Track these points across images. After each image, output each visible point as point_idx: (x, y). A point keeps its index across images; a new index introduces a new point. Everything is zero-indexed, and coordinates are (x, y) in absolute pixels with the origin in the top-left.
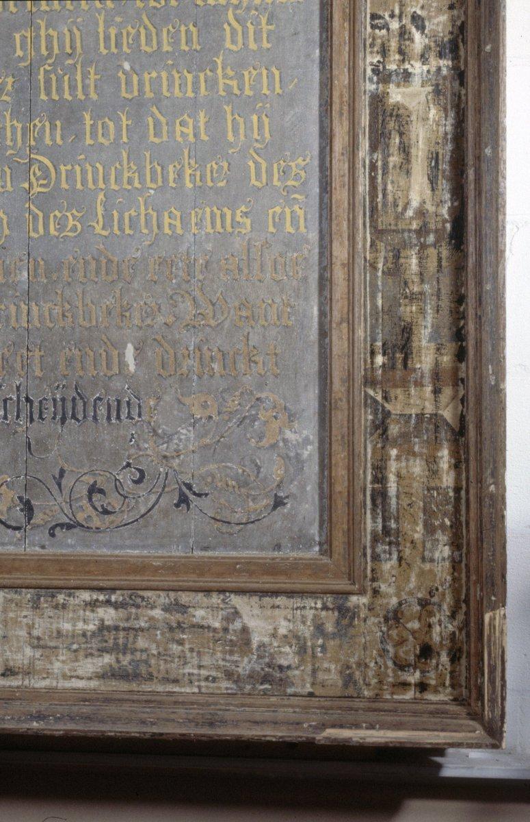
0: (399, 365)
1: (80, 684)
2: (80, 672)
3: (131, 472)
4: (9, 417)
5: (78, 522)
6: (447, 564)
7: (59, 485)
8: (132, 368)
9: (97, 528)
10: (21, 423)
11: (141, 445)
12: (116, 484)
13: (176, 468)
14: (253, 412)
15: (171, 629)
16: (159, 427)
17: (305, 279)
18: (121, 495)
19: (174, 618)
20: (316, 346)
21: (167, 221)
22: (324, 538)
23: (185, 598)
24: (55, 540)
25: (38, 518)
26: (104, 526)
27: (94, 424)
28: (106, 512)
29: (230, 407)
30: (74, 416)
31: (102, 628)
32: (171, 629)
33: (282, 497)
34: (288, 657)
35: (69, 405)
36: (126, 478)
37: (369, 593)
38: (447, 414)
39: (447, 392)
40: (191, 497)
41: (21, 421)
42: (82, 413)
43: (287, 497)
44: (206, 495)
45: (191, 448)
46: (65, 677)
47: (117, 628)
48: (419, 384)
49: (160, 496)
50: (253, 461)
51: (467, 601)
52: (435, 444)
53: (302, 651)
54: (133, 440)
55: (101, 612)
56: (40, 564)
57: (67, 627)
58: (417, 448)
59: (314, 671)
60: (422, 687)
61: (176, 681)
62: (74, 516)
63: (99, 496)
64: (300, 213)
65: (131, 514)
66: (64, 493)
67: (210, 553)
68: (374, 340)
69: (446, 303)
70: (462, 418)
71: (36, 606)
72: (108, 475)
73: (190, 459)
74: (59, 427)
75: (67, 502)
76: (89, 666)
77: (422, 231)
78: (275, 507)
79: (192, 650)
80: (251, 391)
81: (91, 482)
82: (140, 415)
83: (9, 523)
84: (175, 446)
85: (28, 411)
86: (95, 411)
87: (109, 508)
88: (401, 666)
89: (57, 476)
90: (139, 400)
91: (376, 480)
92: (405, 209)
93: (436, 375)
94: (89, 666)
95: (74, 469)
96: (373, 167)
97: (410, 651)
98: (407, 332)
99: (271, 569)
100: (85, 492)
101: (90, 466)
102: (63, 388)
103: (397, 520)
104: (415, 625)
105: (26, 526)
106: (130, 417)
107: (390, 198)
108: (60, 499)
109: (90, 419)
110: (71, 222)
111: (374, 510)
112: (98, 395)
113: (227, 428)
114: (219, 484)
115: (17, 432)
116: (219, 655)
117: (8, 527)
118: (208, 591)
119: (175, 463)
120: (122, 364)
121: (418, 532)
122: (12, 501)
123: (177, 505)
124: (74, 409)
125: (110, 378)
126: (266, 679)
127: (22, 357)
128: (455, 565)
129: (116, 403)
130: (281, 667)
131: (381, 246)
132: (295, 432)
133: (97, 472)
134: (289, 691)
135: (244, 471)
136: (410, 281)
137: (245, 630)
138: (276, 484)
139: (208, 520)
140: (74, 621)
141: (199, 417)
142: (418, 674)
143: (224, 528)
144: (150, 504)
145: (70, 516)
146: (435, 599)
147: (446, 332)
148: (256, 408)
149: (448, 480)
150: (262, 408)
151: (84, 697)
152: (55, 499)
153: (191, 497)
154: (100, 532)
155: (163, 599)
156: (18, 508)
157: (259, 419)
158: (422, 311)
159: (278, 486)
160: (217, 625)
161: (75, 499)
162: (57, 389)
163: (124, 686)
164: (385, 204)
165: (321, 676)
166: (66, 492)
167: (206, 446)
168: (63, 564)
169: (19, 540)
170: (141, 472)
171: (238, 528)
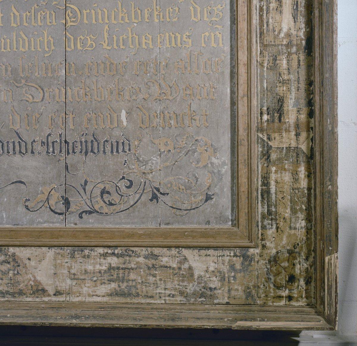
0: (277, 120)
1: (98, 299)
2: (98, 293)
3: (125, 181)
4: (56, 151)
5: (95, 210)
6: (304, 230)
7: (85, 190)
8: (125, 123)
9: (106, 213)
10: (63, 155)
11: (130, 167)
12: (116, 189)
13: (150, 179)
14: (194, 148)
15: (149, 268)
16: (141, 157)
17: (223, 73)
18: (120, 195)
19: (150, 262)
20: (229, 110)
21: (144, 41)
22: (234, 217)
23: (156, 251)
24: (83, 220)
25: (73, 208)
27: (104, 155)
28: (111, 204)
29: (180, 145)
30: (92, 151)
31: (110, 268)
32: (149, 268)
33: (210, 194)
34: (215, 283)
35: (89, 145)
37: (260, 247)
38: (304, 147)
39: (304, 135)
40: (159, 195)
41: (62, 154)
42: (97, 149)
43: (213, 195)
44: (168, 194)
45: (159, 168)
46: (89, 295)
47: (118, 268)
48: (288, 131)
49: (142, 195)
51: (315, 251)
52: (297, 163)
53: (223, 279)
54: (126, 164)
55: (109, 259)
56: (74, 233)
57: (90, 268)
58: (286, 167)
59: (229, 291)
60: (290, 298)
61: (152, 297)
62: (93, 206)
63: (107, 195)
64: (220, 36)
65: (125, 205)
67: (170, 227)
68: (262, 106)
69: (303, 86)
70: (312, 150)
71: (73, 257)
72: (112, 184)
74: (84, 157)
75: (89, 199)
76: (103, 289)
77: (289, 45)
78: (206, 201)
79: (161, 280)
80: (192, 136)
82: (129, 150)
84: (150, 167)
85: (66, 148)
86: (104, 148)
87: (113, 202)
88: (278, 287)
90: (129, 141)
91: (263, 184)
92: (279, 33)
93: (297, 126)
94: (103, 289)
95: (93, 181)
96: (261, 9)
97: (283, 279)
98: (281, 101)
99: (205, 234)
100: (99, 193)
101: (102, 179)
103: (276, 206)
104: (286, 264)
105: (66, 212)
106: (124, 151)
107: (271, 27)
108: (85, 197)
109: (102, 152)
110: (89, 42)
111: (262, 201)
112: (106, 139)
114: (175, 188)
115: (60, 160)
116: (176, 282)
117: (56, 213)
118: (169, 247)
119: (150, 176)
120: (119, 121)
121: (287, 213)
122: (58, 199)
123: (151, 200)
124: (92, 147)
125: (112, 129)
126: (202, 295)
127: (62, 118)
128: (308, 231)
130: (211, 289)
131: (266, 53)
132: (218, 159)
133: (106, 182)
134: (215, 301)
135: (189, 181)
136: (282, 73)
137: (190, 268)
138: (207, 187)
139: (169, 207)
140: (94, 265)
142: (287, 291)
143: (178, 212)
144: (136, 200)
145: (91, 206)
146: (297, 250)
147: (303, 102)
149: (304, 183)
150: (199, 145)
151: (101, 306)
152: (82, 197)
153: (159, 195)
155: (144, 251)
156: (61, 203)
157: (197, 151)
158: (289, 90)
159: (208, 188)
160: (175, 266)
162: (82, 136)
163: (122, 300)
164: (268, 31)
165: (233, 293)
166: (88, 193)
167: (167, 167)
168: (86, 233)
169: (62, 220)
170: (131, 181)
171: (186, 212)
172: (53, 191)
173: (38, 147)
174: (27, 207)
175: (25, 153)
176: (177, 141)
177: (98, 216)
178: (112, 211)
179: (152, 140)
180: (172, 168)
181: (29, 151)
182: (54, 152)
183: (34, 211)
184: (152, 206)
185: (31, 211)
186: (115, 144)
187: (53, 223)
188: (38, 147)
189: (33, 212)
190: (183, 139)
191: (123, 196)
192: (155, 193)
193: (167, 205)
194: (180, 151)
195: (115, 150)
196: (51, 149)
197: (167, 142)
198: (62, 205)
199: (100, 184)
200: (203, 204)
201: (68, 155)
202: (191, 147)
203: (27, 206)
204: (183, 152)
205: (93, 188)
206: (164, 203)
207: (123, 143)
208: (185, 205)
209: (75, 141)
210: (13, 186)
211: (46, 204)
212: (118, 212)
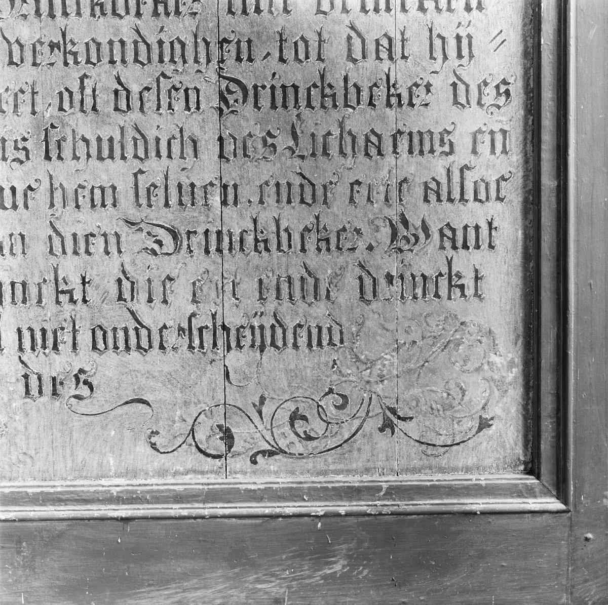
3: (334, 397)
4: (205, 345)
5: (281, 449)
9: (300, 454)
10: (219, 351)
11: (343, 371)
12: (318, 410)
13: (380, 393)
14: (458, 337)
16: (362, 353)
18: (324, 421)
22: (529, 457)
24: (257, 467)
26: (307, 451)
27: (295, 351)
28: (309, 438)
30: (273, 344)
35: (268, 333)
36: (329, 403)
40: (395, 421)
41: (218, 349)
42: (281, 340)
43: (492, 419)
44: (411, 418)
45: (395, 372)
49: (364, 420)
50: (458, 385)
54: (336, 366)
62: (276, 442)
63: (301, 422)
65: (334, 439)
66: (265, 420)
72: (311, 402)
73: (394, 384)
74: (258, 354)
78: (480, 429)
81: (293, 408)
82: (342, 342)
83: (208, 451)
84: (379, 372)
85: (225, 339)
86: (295, 338)
87: (313, 435)
89: (258, 404)
90: (341, 326)
101: (292, 393)
102: (261, 316)
105: (226, 454)
106: (331, 343)
108: (261, 427)
109: (290, 345)
112: (298, 322)
113: (431, 353)
114: (424, 408)
117: (208, 455)
122: (212, 429)
123: (381, 430)
124: (273, 336)
127: (217, 284)
129: (317, 330)
133: (299, 399)
135: (449, 394)
138: (481, 406)
139: (413, 443)
141: (403, 342)
144: (354, 429)
145: (272, 443)
148: (460, 333)
150: (466, 332)
152: (255, 426)
153: (395, 421)
154: (303, 458)
156: (218, 437)
159: (483, 408)
161: (277, 426)
162: (255, 317)
167: (409, 371)
169: (220, 468)
170: (344, 397)
171: (443, 450)
172: (202, 416)
173: (171, 338)
174: (153, 446)
175: (147, 348)
176: (428, 325)
177: (286, 460)
178: (311, 450)
179: (383, 323)
180: (420, 372)
181: (156, 344)
182: (202, 346)
183: (168, 452)
184: (383, 441)
185: (161, 453)
186: (315, 331)
187: (202, 473)
188: (171, 338)
189: (165, 455)
190: (439, 321)
191: (330, 423)
192: (388, 417)
193: (411, 437)
194: (434, 342)
195: (315, 343)
196: (197, 342)
197: (410, 327)
198: (219, 441)
199: (289, 402)
200: (474, 436)
201: (228, 351)
202: (453, 335)
203: (155, 444)
204: (439, 345)
205: (276, 410)
206: (405, 434)
207: (330, 330)
208: (442, 438)
209: (242, 327)
210: (126, 407)
211: (190, 439)
212: (322, 452)
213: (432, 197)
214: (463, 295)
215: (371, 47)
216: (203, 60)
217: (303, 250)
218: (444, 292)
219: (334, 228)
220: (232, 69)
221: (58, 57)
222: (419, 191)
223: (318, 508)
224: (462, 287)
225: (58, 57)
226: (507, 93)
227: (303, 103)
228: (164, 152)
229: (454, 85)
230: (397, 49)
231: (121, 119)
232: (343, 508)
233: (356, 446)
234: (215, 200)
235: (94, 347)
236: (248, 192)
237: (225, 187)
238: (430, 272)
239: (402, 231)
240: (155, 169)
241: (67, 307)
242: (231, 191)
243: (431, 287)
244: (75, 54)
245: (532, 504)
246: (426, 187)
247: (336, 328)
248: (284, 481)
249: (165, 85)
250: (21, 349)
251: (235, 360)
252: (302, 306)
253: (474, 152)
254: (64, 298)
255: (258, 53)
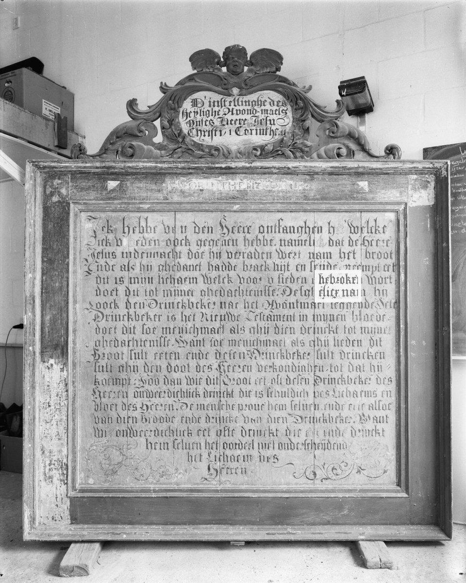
7: (324, 467)
28: (337, 475)
35: (326, 445)
36: (343, 465)
106: (343, 448)
123: (357, 473)
166: (326, 469)
170: (347, 463)
173: (300, 446)
174: (294, 476)
181: (296, 448)
184: (357, 476)
187: (308, 484)
196: (307, 447)
207: (343, 444)
210: (287, 465)
211: (304, 475)
213: (371, 409)
214: (379, 435)
215: (355, 368)
216: (310, 371)
217: (336, 422)
218: (374, 434)
219: (344, 417)
220: (317, 373)
221: (271, 370)
222: (367, 407)
223: (340, 495)
224: (379, 433)
225: (271, 370)
226: (391, 381)
227: (336, 382)
228: (299, 396)
229: (377, 378)
230: (362, 369)
231: (288, 386)
232: (347, 495)
233: (350, 477)
234: (312, 408)
235: (279, 448)
236: (322, 407)
237: (315, 405)
238: (371, 429)
239: (363, 418)
240: (297, 400)
241: (272, 437)
242: (317, 406)
243: (370, 433)
244: (276, 369)
245: (399, 495)
246: (369, 406)
247: (345, 444)
248: (330, 487)
249: (300, 378)
250: (259, 449)
251: (317, 452)
252: (335, 438)
253: (382, 396)
254: (271, 435)
255: (325, 369)
